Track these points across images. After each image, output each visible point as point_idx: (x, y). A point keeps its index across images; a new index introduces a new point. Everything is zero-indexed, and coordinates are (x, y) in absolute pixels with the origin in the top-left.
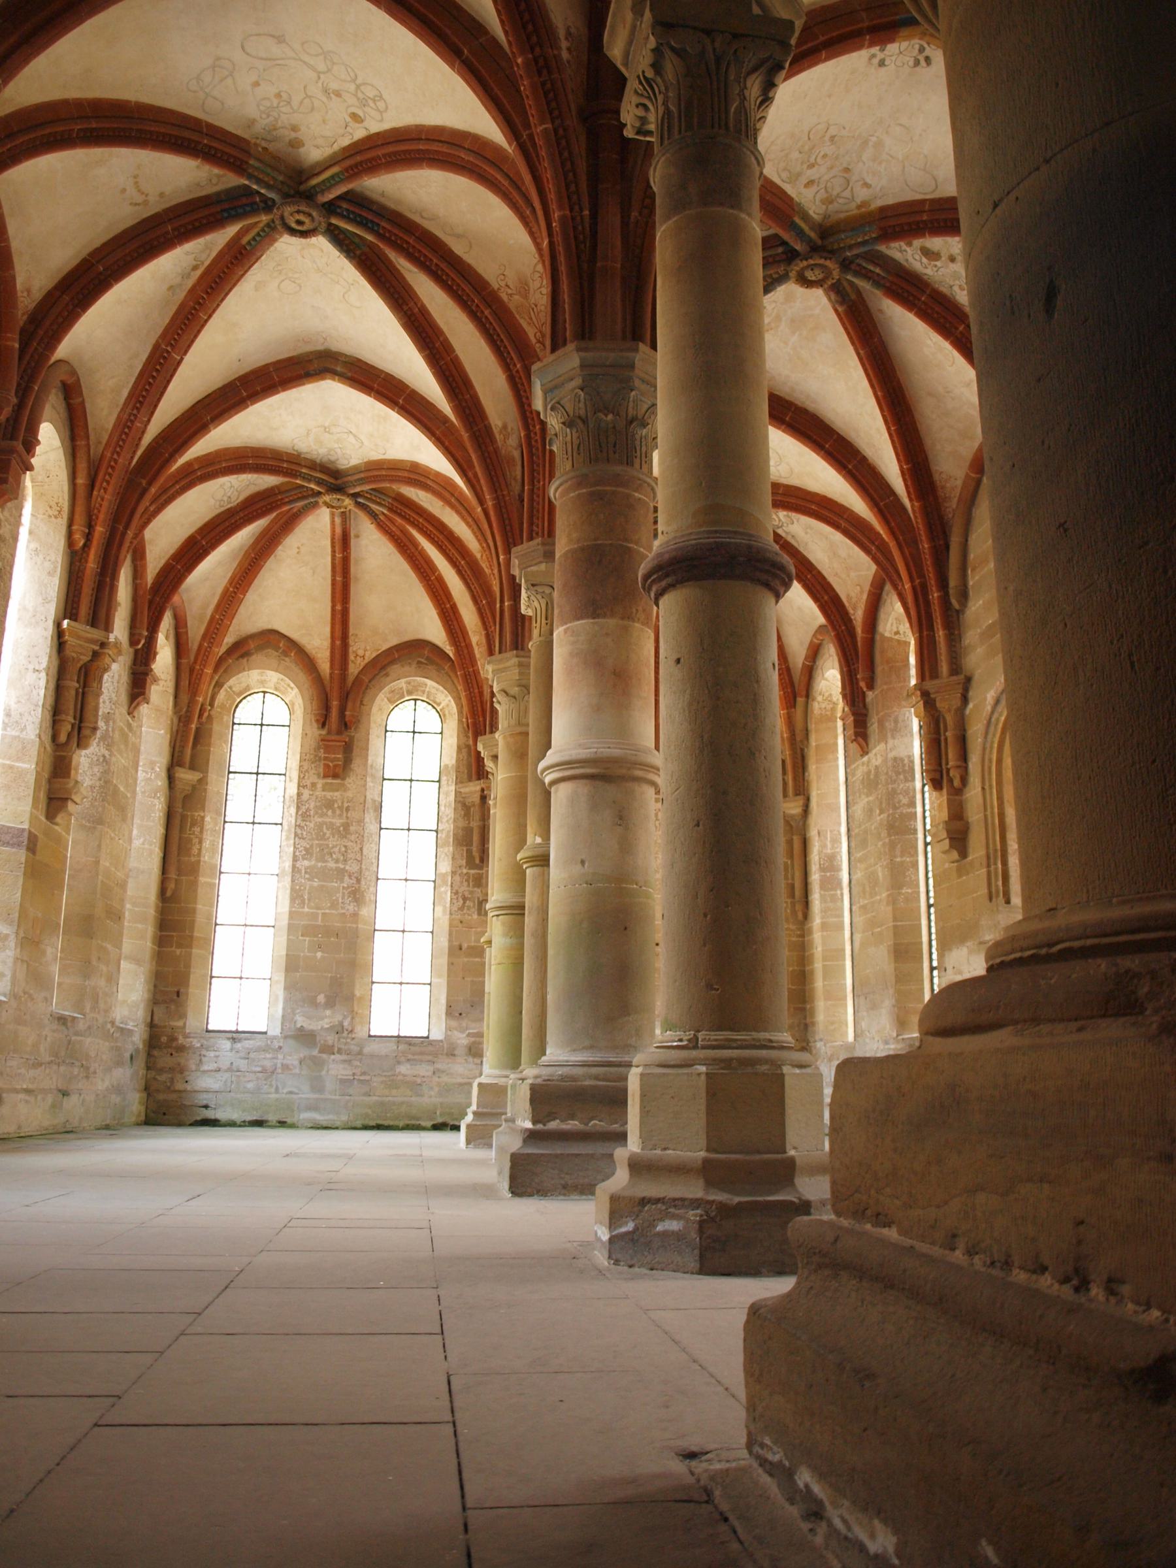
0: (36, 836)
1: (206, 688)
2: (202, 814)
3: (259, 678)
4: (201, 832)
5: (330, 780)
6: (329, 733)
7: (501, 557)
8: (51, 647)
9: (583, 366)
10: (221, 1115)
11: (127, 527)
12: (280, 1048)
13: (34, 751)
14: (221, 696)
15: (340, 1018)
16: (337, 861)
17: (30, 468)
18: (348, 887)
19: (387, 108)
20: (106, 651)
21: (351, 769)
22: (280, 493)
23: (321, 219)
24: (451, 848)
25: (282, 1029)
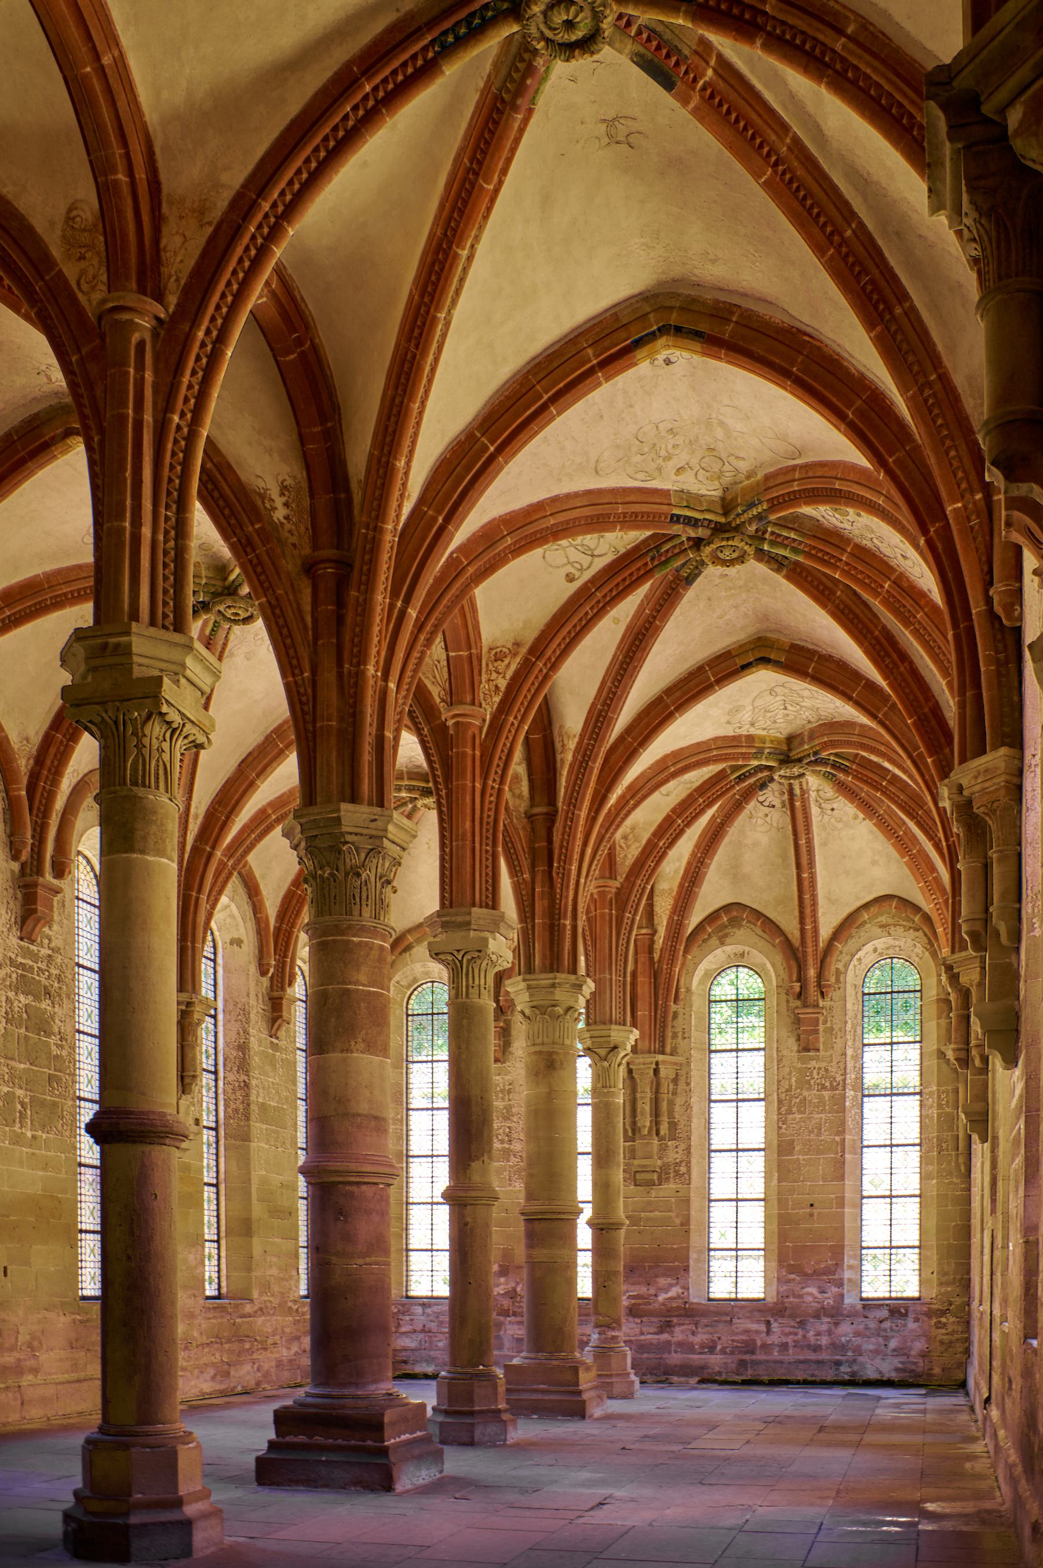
10: (419, 1369)
11: (200, 891)
15: (513, 1284)
16: (502, 1142)
21: (511, 1053)
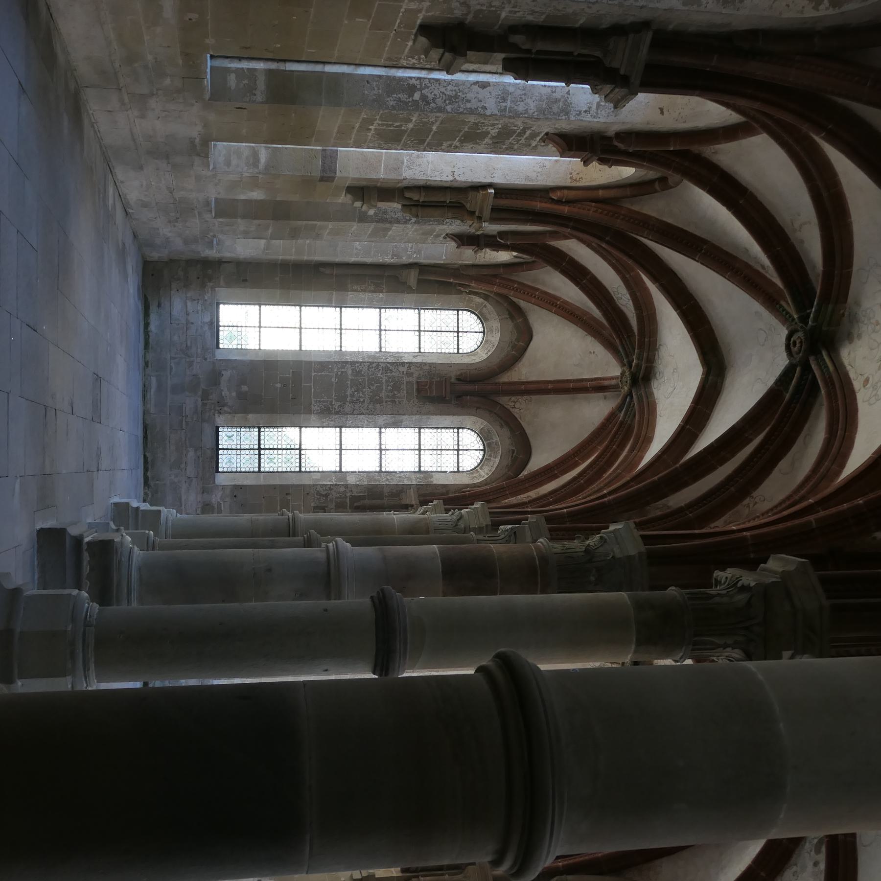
0: (333, 181)
1: (483, 288)
2: (384, 291)
3: (494, 328)
4: (370, 291)
5: (415, 386)
6: (452, 384)
7: (565, 510)
8: (473, 182)
9: (630, 558)
10: (153, 318)
12: (206, 359)
13: (393, 176)
14: (478, 300)
16: (352, 395)
17: (586, 162)
18: (332, 405)
19: (870, 405)
20: (476, 221)
22: (629, 337)
23: (798, 360)
24: (366, 483)
25: (220, 360)
